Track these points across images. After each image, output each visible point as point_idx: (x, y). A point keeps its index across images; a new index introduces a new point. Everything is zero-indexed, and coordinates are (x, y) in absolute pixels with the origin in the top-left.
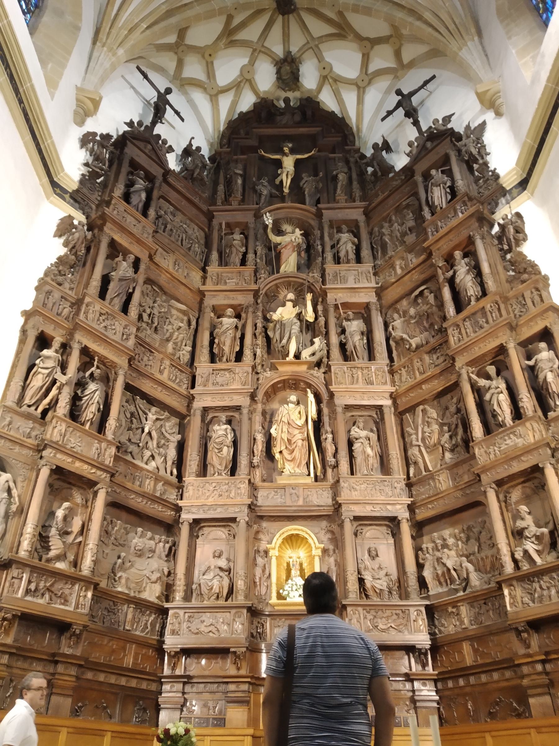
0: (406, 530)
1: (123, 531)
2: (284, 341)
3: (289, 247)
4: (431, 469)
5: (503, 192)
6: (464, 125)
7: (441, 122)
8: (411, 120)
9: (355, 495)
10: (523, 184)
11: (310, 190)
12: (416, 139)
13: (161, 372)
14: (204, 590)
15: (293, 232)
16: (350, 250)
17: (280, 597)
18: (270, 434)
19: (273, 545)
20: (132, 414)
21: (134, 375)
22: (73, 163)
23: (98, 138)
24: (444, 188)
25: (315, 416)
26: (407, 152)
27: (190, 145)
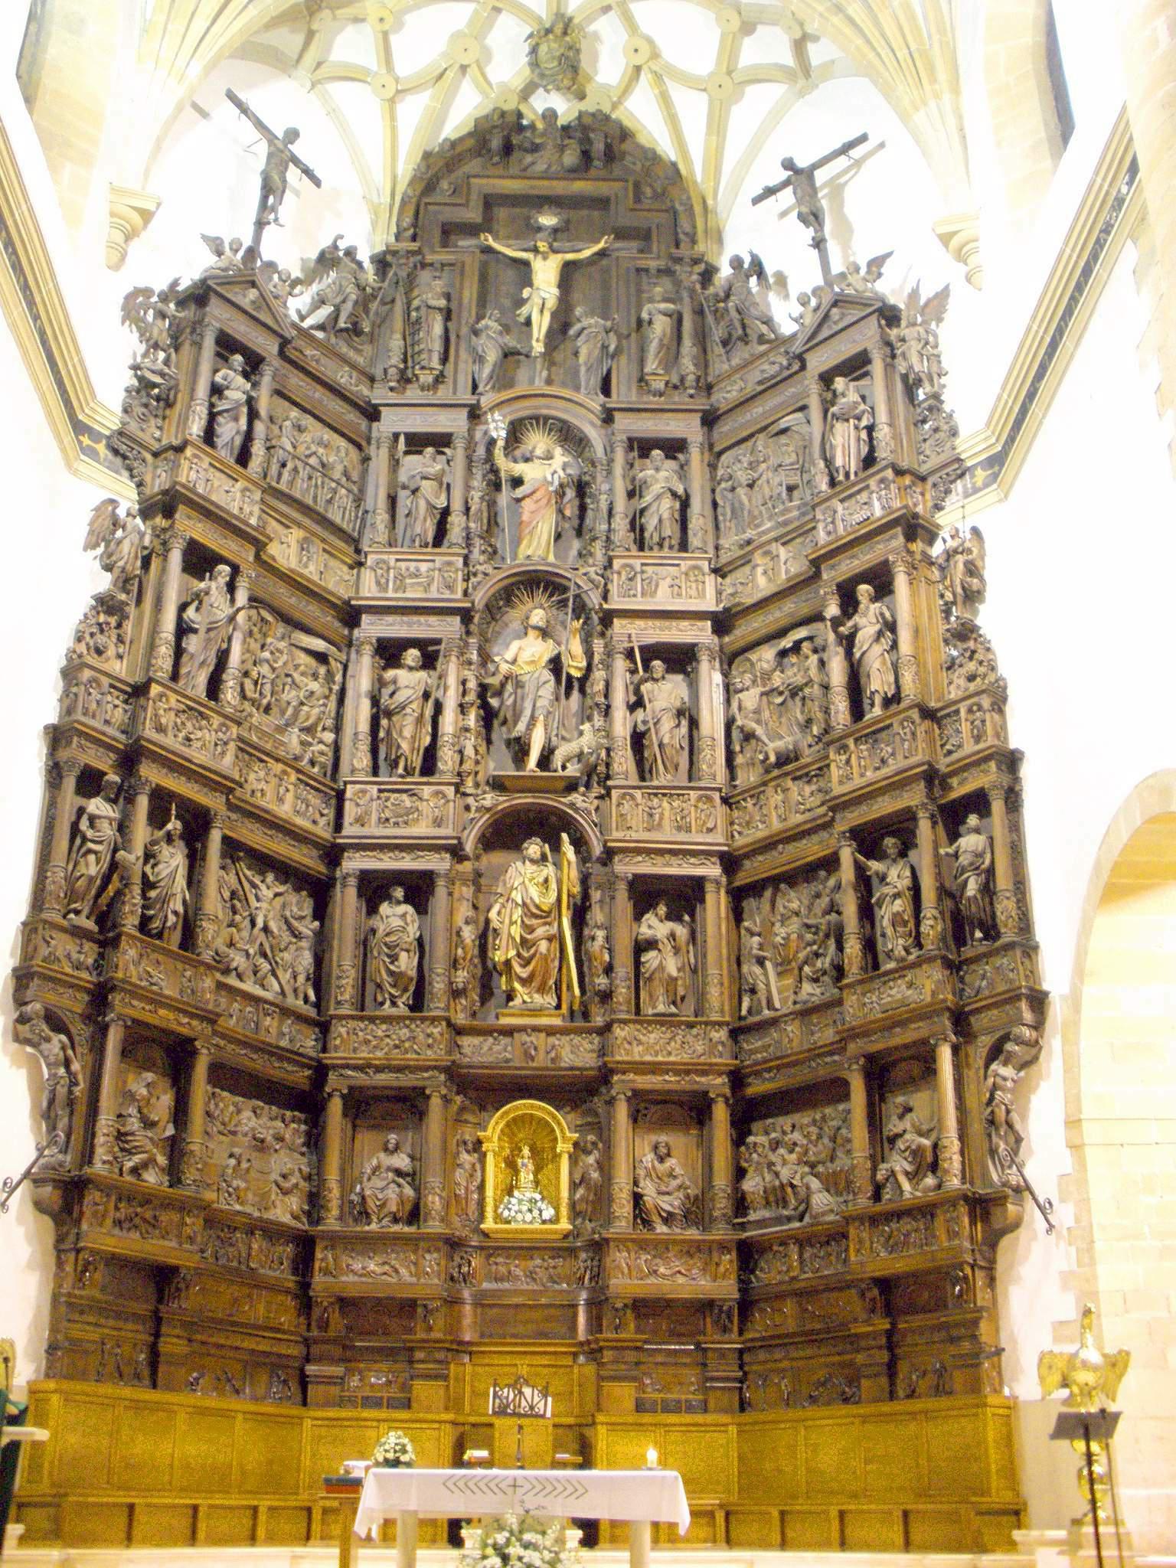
0: (721, 1113)
1: (231, 1108)
2: (521, 727)
3: (538, 495)
4: (777, 1005)
5: (957, 469)
6: (908, 290)
7: (863, 271)
8: (810, 232)
9: (637, 1054)
10: (996, 461)
11: (589, 355)
13: (281, 800)
14: (371, 1205)
15: (549, 456)
16: (666, 516)
17: (498, 1218)
18: (487, 921)
19: (489, 1132)
20: (233, 894)
21: (234, 816)
22: (111, 361)
23: (155, 299)
24: (856, 428)
25: (577, 890)
26: (795, 315)
27: (335, 247)
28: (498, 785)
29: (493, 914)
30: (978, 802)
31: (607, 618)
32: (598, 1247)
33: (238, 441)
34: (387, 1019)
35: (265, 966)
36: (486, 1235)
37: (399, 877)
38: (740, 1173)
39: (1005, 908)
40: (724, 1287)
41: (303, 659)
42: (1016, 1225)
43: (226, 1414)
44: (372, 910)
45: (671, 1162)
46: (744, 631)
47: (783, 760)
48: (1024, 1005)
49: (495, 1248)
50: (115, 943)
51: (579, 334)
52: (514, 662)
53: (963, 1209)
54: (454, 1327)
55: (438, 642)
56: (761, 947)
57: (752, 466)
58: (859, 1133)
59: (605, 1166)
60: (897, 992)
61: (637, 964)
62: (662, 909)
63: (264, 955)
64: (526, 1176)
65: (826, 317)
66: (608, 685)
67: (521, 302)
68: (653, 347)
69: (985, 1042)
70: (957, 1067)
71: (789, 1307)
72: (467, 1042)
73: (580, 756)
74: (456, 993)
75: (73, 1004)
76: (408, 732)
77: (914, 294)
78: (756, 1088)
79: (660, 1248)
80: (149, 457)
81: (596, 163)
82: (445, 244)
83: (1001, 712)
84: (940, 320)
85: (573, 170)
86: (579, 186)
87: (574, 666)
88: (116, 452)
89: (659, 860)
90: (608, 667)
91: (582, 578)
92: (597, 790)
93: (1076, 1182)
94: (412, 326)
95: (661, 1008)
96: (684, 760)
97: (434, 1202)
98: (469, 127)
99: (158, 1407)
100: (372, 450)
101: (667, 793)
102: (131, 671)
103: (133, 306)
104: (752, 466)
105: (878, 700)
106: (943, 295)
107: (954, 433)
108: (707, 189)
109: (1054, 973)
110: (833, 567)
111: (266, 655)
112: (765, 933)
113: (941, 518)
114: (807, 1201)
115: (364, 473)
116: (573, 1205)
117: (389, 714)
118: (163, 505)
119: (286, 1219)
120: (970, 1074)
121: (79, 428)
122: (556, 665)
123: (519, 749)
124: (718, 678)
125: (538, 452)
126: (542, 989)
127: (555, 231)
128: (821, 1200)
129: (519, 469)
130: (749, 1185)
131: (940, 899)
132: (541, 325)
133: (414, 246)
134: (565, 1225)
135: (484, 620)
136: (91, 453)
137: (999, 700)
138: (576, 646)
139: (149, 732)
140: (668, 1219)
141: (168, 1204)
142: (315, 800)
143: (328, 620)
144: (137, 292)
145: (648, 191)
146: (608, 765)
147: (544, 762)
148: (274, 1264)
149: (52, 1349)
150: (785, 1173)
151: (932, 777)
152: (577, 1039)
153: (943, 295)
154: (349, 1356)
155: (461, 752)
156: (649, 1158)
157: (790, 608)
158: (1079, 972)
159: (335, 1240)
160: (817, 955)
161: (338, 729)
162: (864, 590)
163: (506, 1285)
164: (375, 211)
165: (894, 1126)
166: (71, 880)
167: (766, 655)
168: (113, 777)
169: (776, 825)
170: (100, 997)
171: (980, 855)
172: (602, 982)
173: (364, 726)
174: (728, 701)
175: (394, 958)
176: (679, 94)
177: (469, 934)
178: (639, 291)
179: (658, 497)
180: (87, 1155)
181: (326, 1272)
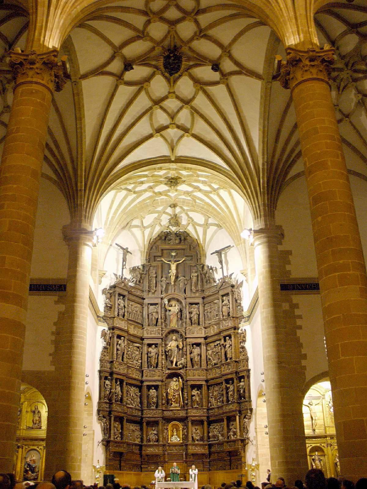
0: (205, 423)
2: (172, 358)
9: (192, 414)
10: (249, 317)
12: (221, 278)
14: (151, 440)
17: (171, 441)
20: (127, 391)
25: (182, 386)
28: (169, 369)
29: (168, 391)
30: (243, 377)
31: (186, 338)
32: (186, 445)
33: (123, 314)
34: (152, 410)
35: (132, 402)
36: (169, 443)
37: (153, 386)
38: (209, 432)
39: (247, 395)
40: (207, 452)
41: (135, 348)
42: (248, 443)
43: (131, 474)
44: (149, 391)
45: (198, 431)
46: (209, 340)
47: (215, 364)
48: (249, 411)
49: (170, 445)
50: (112, 404)
51: (180, 280)
52: (170, 346)
53: (240, 441)
54: (164, 458)
55: (157, 344)
56: (212, 395)
57: (211, 308)
58: (225, 427)
59: (187, 432)
60: (231, 407)
61: (192, 399)
62: (196, 389)
63: (132, 400)
64: (175, 433)
65: (222, 285)
66: (186, 350)
67: (169, 273)
68: (193, 284)
69: (243, 415)
70: (239, 419)
71: (216, 455)
72: (165, 412)
73: (182, 364)
74: (163, 404)
75: (106, 414)
76: (153, 361)
77: (237, 281)
78: (211, 419)
79: (196, 445)
81: (182, 241)
82: (155, 261)
83: (248, 362)
84: (241, 287)
87: (181, 347)
89: (195, 382)
90: (186, 347)
91: (182, 330)
92: (185, 369)
93: (256, 438)
94: (150, 281)
95: (196, 406)
96: (199, 363)
97: (161, 439)
98: (157, 235)
99: (121, 473)
100: (144, 306)
101: (196, 370)
102: (110, 359)
103: (104, 292)
104: (211, 308)
105: (229, 358)
106: (242, 283)
107: (243, 310)
108: (203, 245)
109: (254, 407)
110: (223, 333)
111: (129, 350)
112: (213, 393)
113: (240, 325)
114: (218, 437)
115: (143, 310)
116: (183, 438)
117: (150, 357)
118: (112, 328)
119: (138, 443)
120: (241, 420)
121: (98, 317)
122: (178, 347)
123: (172, 362)
124: (205, 347)
125: (173, 305)
126: (177, 403)
127: (175, 256)
128: (221, 438)
129: (170, 308)
130: (210, 434)
131: (237, 392)
132: (173, 278)
133: (149, 264)
134: (181, 442)
135: (165, 339)
136: (100, 321)
137: (247, 360)
138: (181, 343)
139: (114, 370)
140: (198, 440)
141: (122, 443)
142: (138, 372)
143: (139, 340)
145: (192, 247)
146: (187, 364)
147: (176, 365)
148: (136, 450)
149: (106, 465)
150: (215, 433)
151: (236, 373)
152: (182, 411)
153: (242, 283)
154: (148, 463)
155: (162, 363)
156: (194, 430)
157: (216, 338)
158: (256, 407)
159: (146, 446)
160: (220, 398)
161: (141, 359)
162: (227, 338)
163: (172, 451)
164: (141, 252)
165: (231, 427)
166: (105, 395)
167: (212, 345)
168: (109, 377)
169: (214, 376)
170: (110, 413)
171: (243, 386)
172: (186, 402)
173: (146, 360)
174: (206, 353)
175: (153, 399)
176: (197, 227)
177: (164, 394)
178: (191, 270)
179: (194, 315)
180: (110, 437)
181: (144, 451)
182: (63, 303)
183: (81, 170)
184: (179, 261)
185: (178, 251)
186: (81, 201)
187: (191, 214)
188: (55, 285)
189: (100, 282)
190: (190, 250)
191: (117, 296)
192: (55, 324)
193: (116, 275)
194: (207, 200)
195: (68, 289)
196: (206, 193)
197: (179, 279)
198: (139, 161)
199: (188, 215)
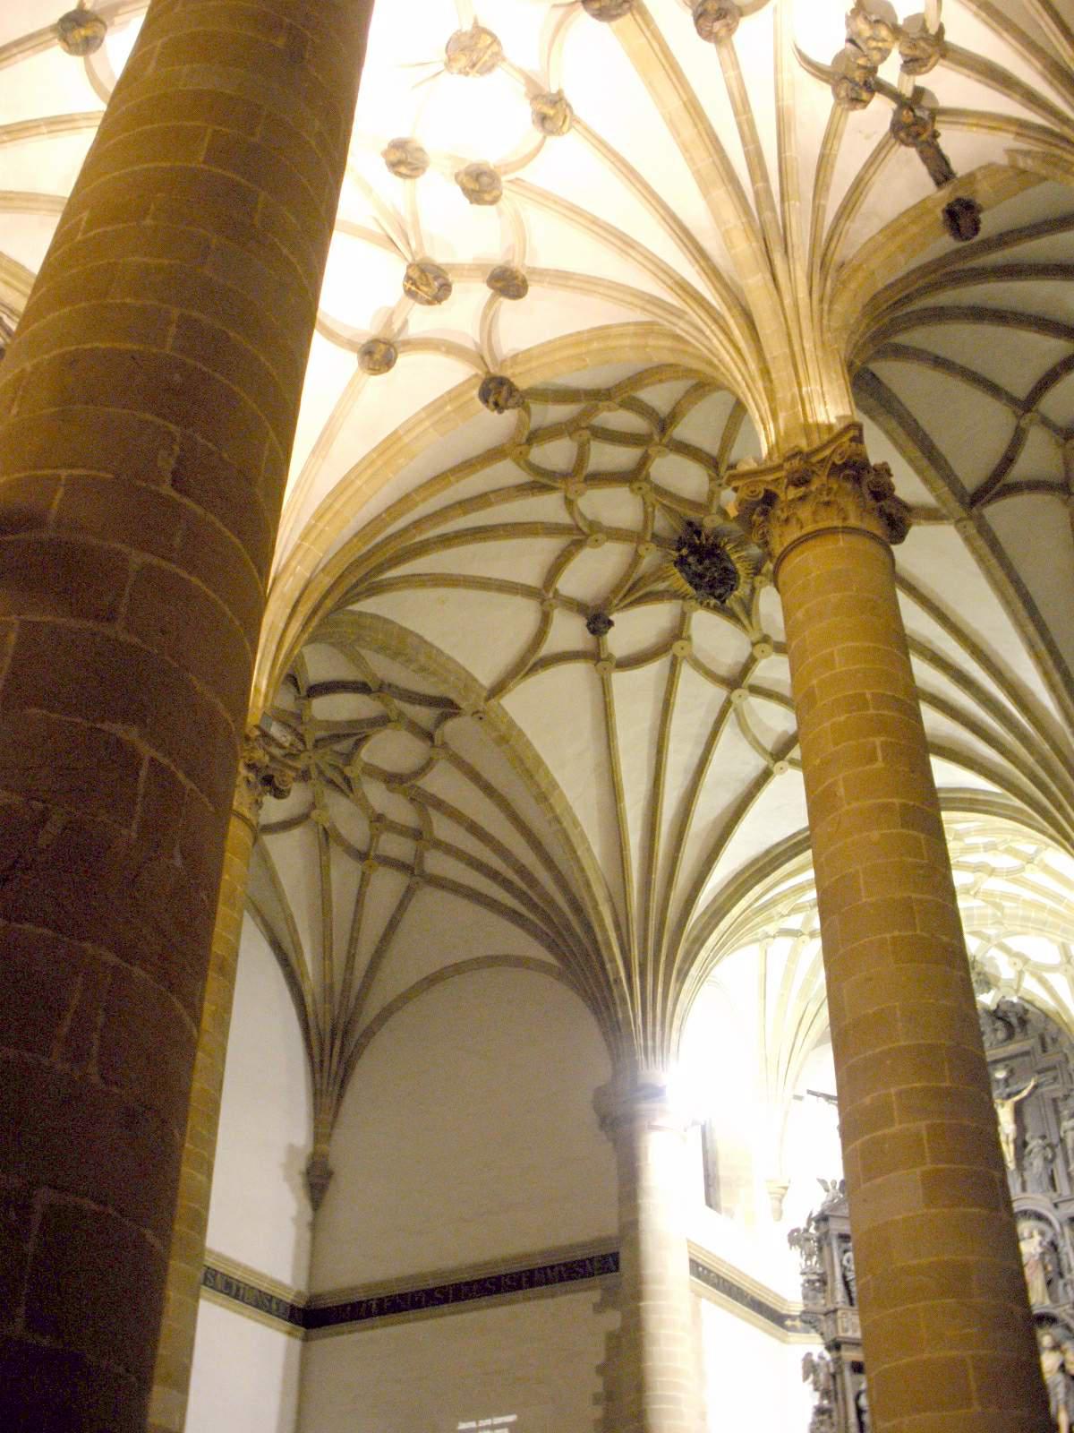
80: (822, 1317)
81: (1018, 1030)
85: (1005, 1040)
86: (1013, 1048)
88: (805, 1322)
144: (793, 1231)
182: (614, 1305)
183: (603, 927)
184: (1019, 1092)
185: (1014, 1063)
186: (625, 1012)
187: (1015, 943)
188: (591, 1260)
189: (779, 1214)
190: (1044, 1050)
191: (835, 1244)
192: (601, 1370)
193: (823, 1182)
194: (1027, 894)
195: (622, 1264)
196: (1012, 875)
197: (1029, 1147)
198: (768, 852)
199: (1003, 948)
